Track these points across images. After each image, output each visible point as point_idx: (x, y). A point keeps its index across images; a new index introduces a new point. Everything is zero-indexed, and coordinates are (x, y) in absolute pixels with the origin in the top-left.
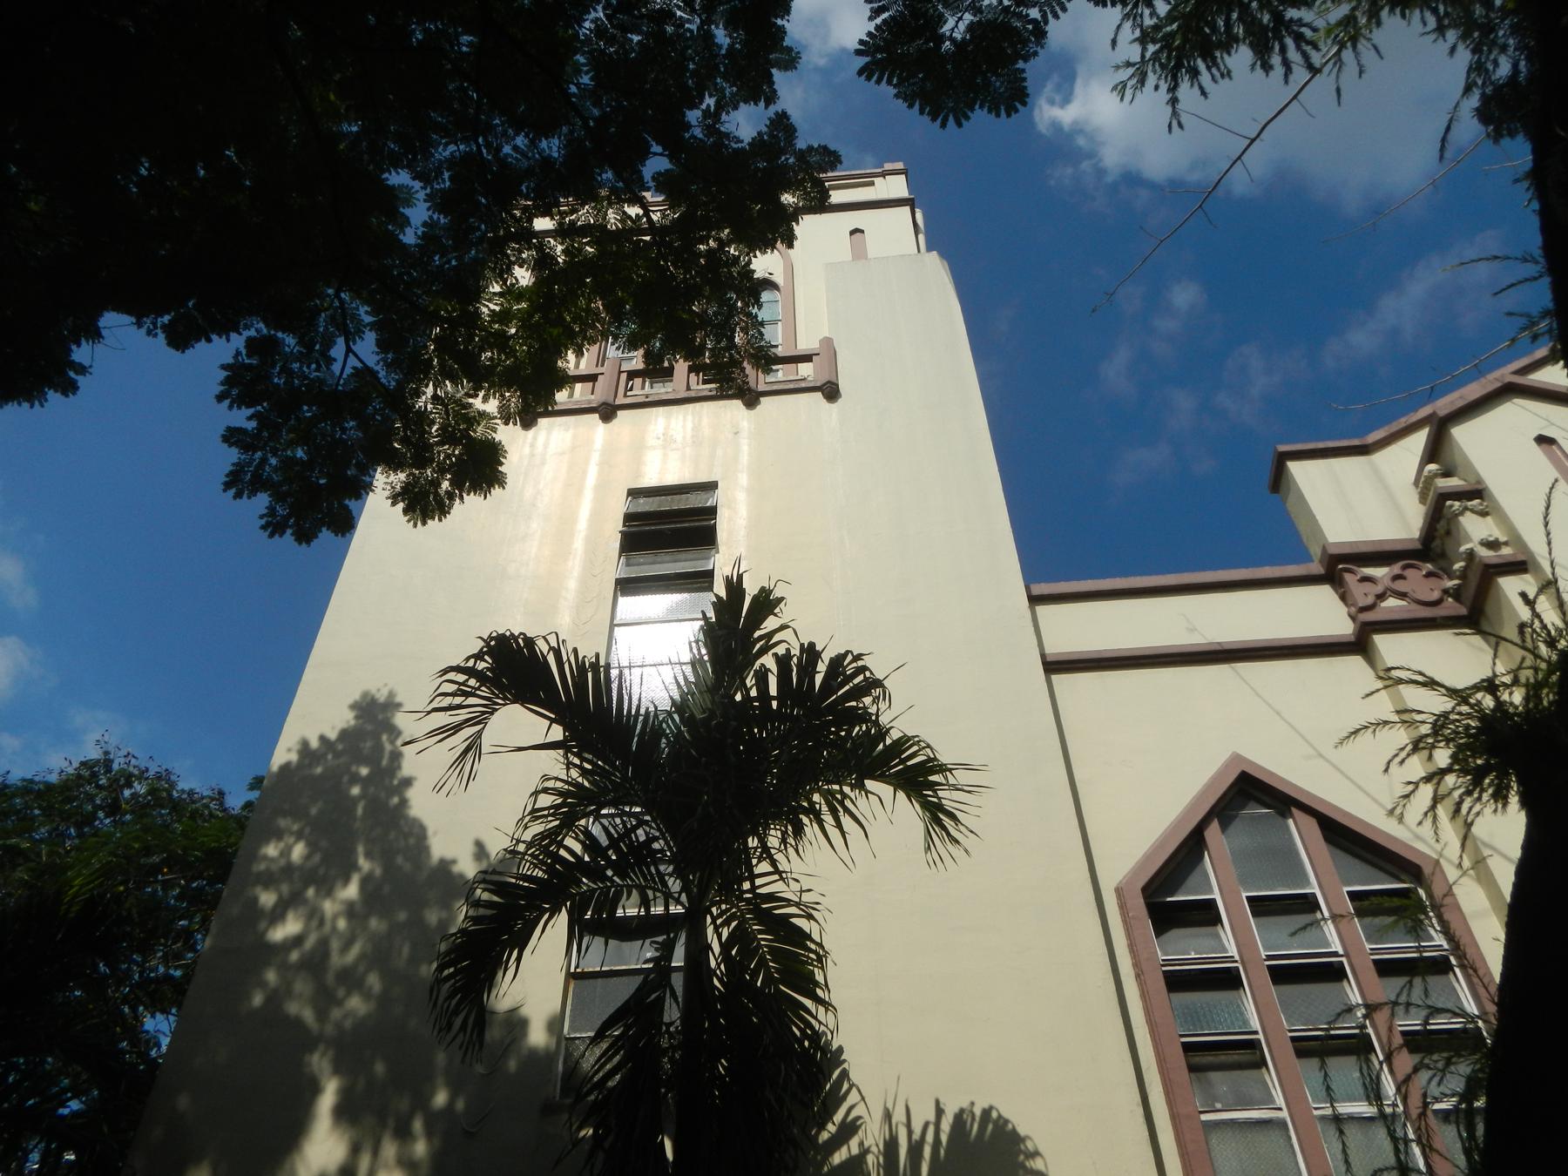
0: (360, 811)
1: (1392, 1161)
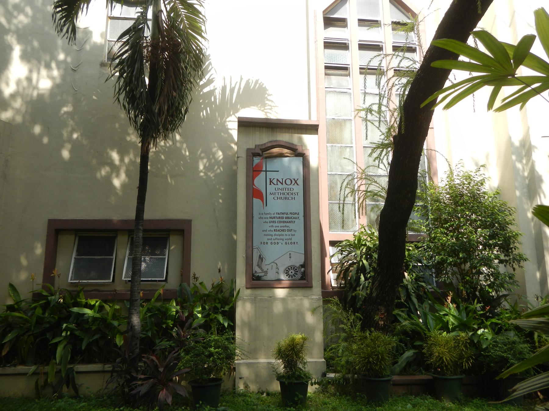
1: (377, 102)
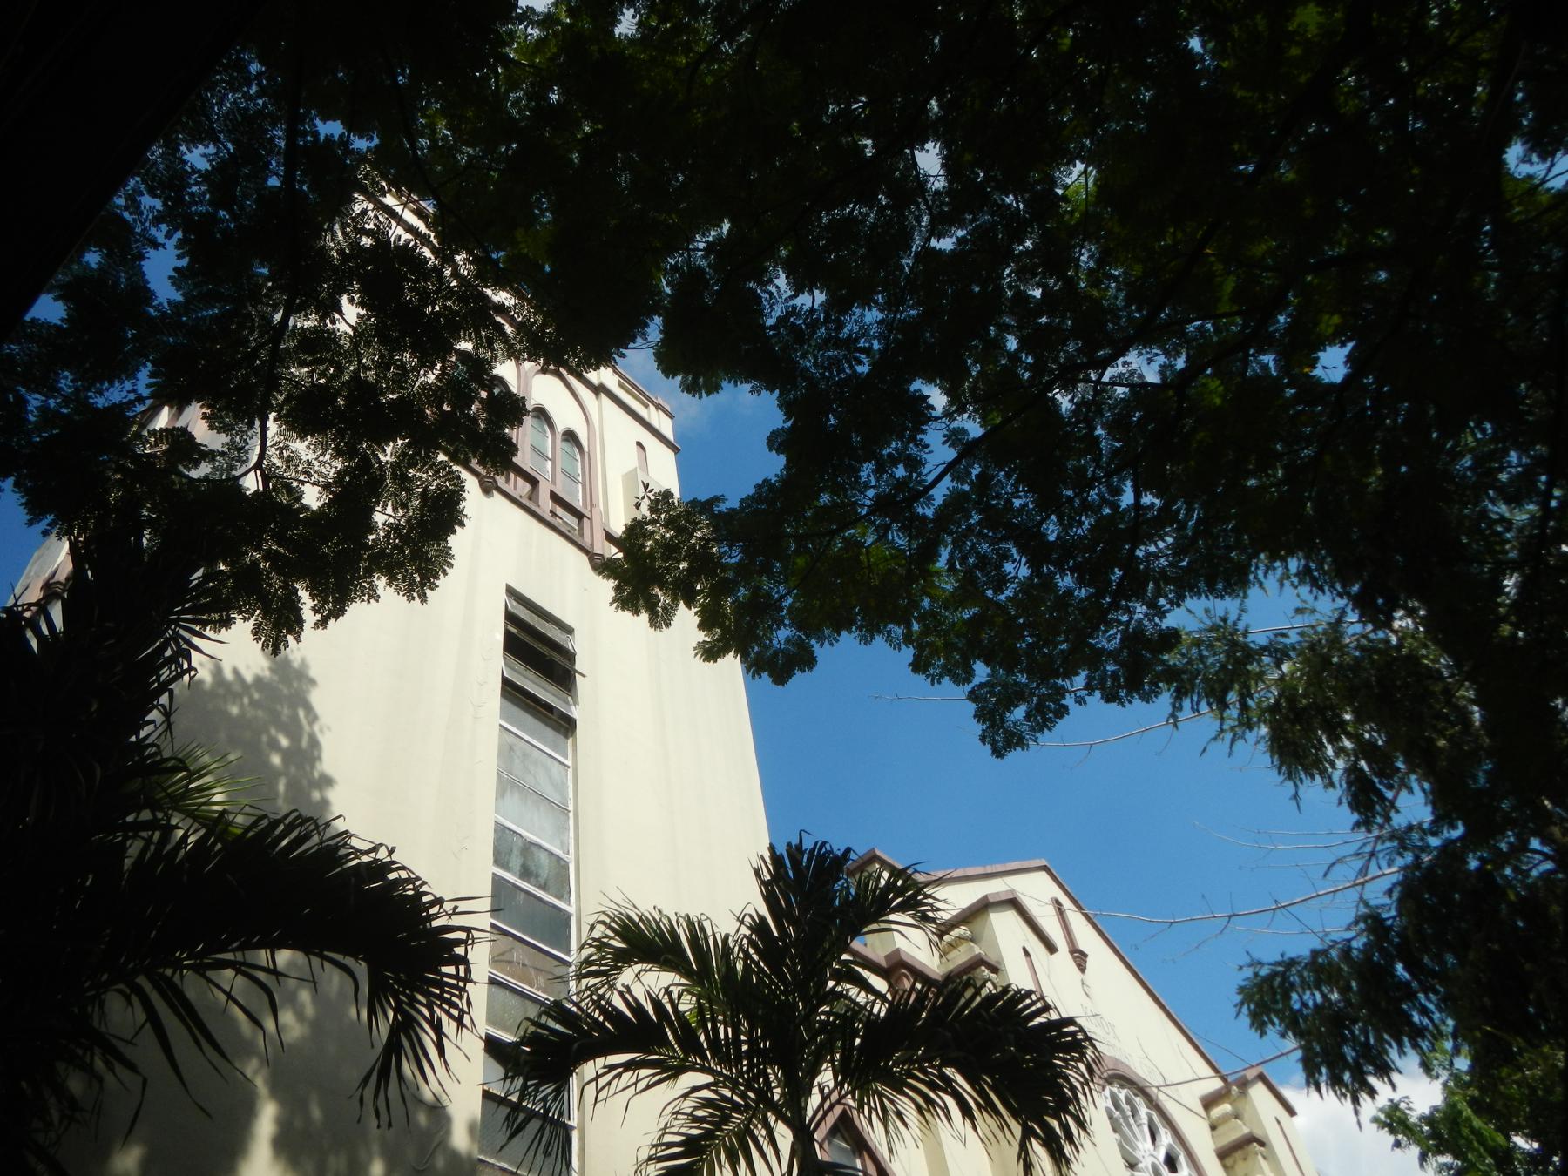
0: (282, 787)
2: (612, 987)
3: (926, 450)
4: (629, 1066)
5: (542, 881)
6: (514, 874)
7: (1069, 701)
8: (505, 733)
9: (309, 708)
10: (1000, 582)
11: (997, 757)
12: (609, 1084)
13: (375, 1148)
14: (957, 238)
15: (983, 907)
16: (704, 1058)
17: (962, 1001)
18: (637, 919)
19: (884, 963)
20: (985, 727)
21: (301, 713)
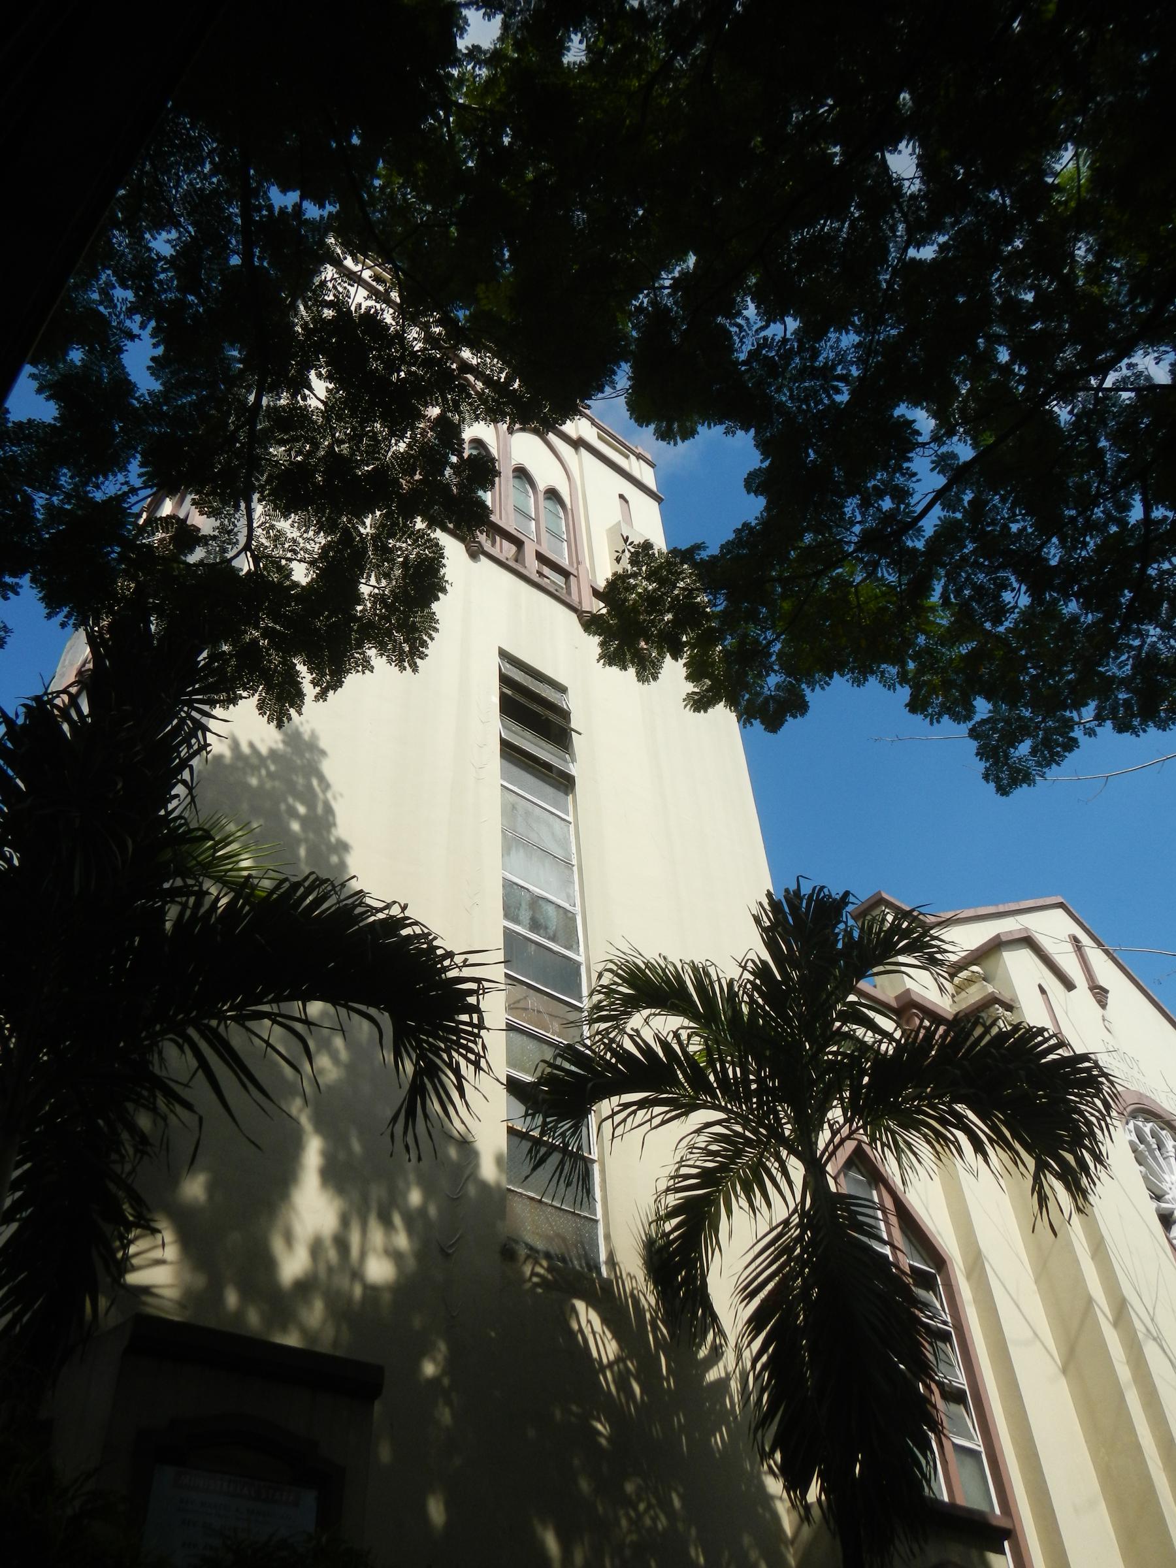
0: (302, 852)
2: (622, 1031)
3: (914, 479)
4: (642, 1104)
5: (551, 932)
6: (524, 927)
7: (1077, 733)
8: (506, 792)
9: (322, 778)
10: (999, 612)
11: (1002, 795)
12: (624, 1120)
13: (412, 1177)
14: (939, 245)
15: (996, 946)
16: (714, 1096)
17: (972, 1039)
18: (643, 967)
19: (894, 1004)
20: (988, 764)
21: (315, 782)
